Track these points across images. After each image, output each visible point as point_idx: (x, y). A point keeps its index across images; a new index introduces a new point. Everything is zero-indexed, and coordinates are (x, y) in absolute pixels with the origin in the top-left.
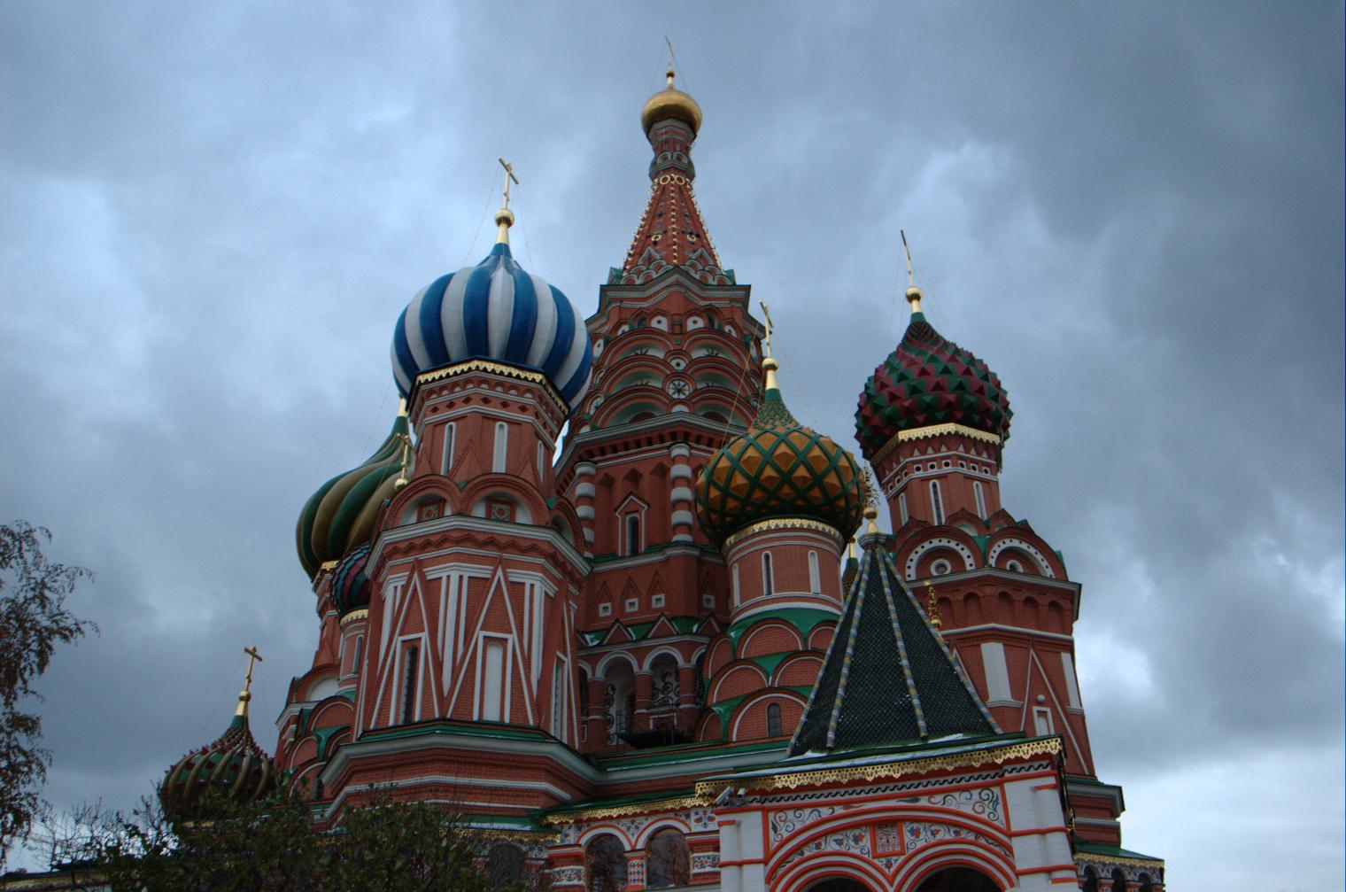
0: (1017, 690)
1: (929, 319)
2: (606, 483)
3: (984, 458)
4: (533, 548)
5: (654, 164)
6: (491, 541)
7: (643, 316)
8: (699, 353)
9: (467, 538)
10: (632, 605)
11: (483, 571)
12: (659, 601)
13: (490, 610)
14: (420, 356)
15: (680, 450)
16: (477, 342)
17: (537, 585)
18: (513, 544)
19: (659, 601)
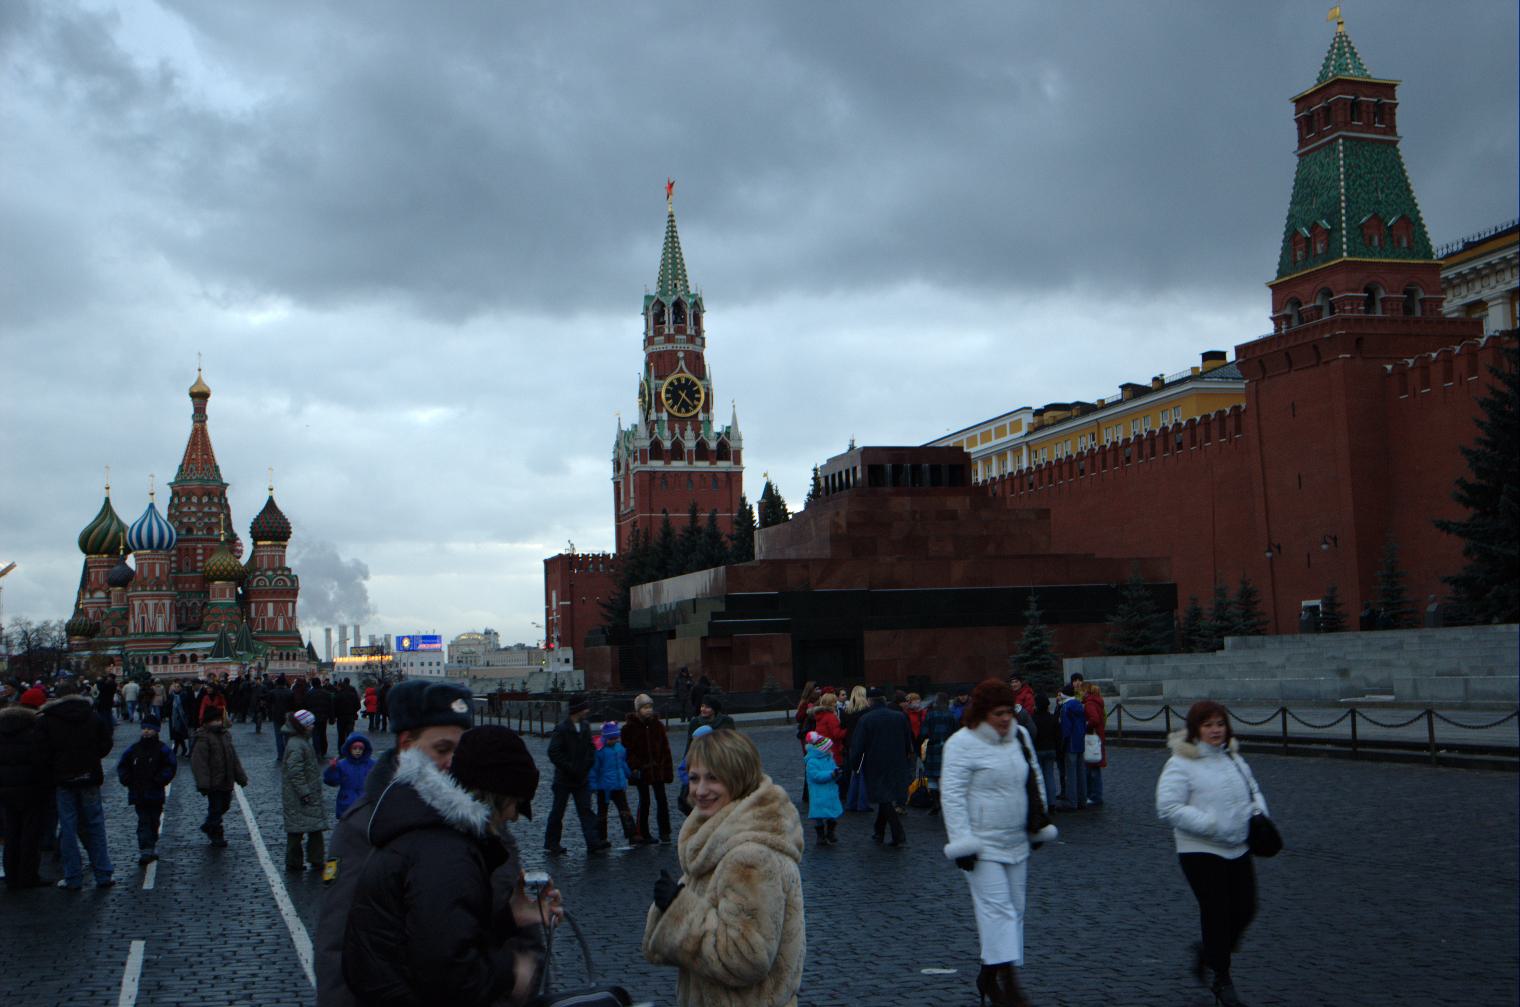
0: (275, 614)
1: (274, 498)
2: (179, 550)
3: (280, 548)
4: (167, 595)
5: (193, 416)
6: (158, 596)
7: (189, 494)
8: (206, 509)
9: (153, 596)
10: (187, 586)
11: (156, 601)
12: (194, 586)
13: (158, 610)
14: (136, 545)
15: (200, 546)
16: (150, 546)
17: (167, 602)
18: (163, 595)
19: (194, 586)
